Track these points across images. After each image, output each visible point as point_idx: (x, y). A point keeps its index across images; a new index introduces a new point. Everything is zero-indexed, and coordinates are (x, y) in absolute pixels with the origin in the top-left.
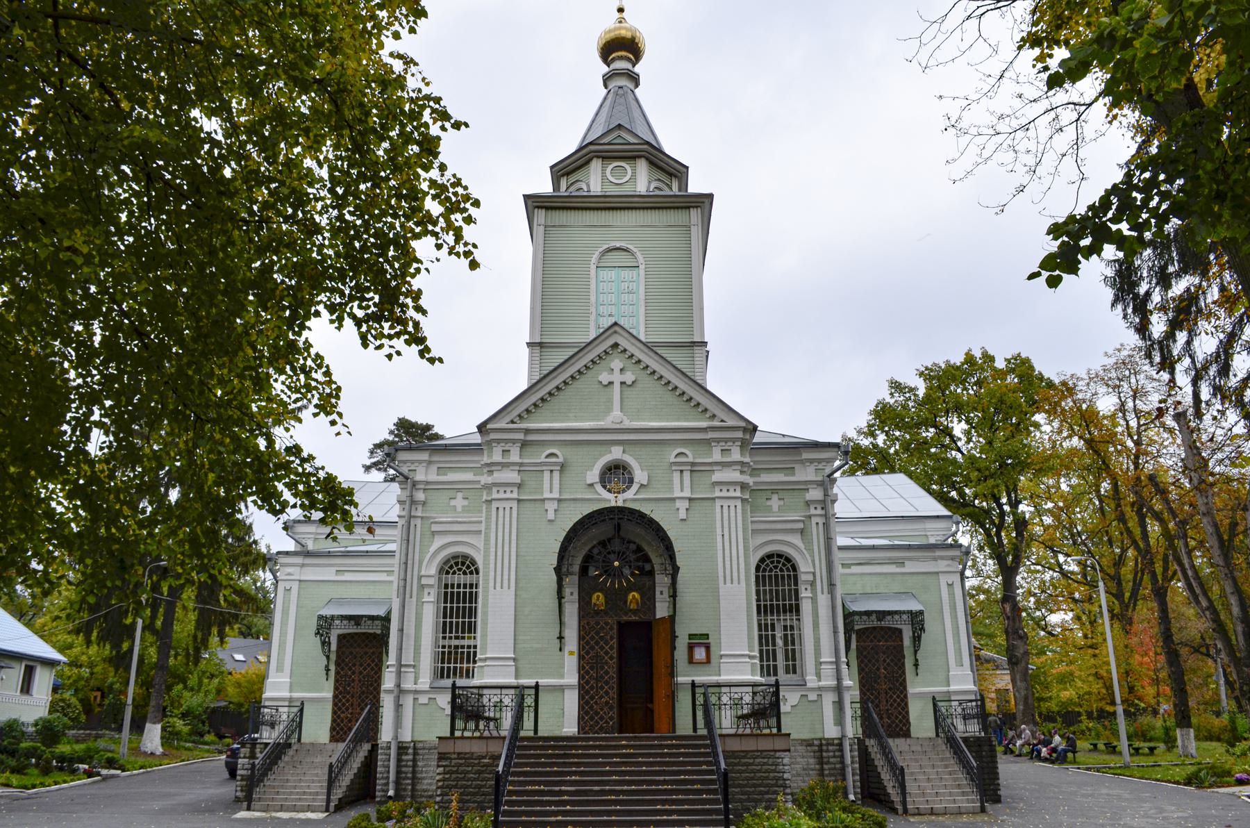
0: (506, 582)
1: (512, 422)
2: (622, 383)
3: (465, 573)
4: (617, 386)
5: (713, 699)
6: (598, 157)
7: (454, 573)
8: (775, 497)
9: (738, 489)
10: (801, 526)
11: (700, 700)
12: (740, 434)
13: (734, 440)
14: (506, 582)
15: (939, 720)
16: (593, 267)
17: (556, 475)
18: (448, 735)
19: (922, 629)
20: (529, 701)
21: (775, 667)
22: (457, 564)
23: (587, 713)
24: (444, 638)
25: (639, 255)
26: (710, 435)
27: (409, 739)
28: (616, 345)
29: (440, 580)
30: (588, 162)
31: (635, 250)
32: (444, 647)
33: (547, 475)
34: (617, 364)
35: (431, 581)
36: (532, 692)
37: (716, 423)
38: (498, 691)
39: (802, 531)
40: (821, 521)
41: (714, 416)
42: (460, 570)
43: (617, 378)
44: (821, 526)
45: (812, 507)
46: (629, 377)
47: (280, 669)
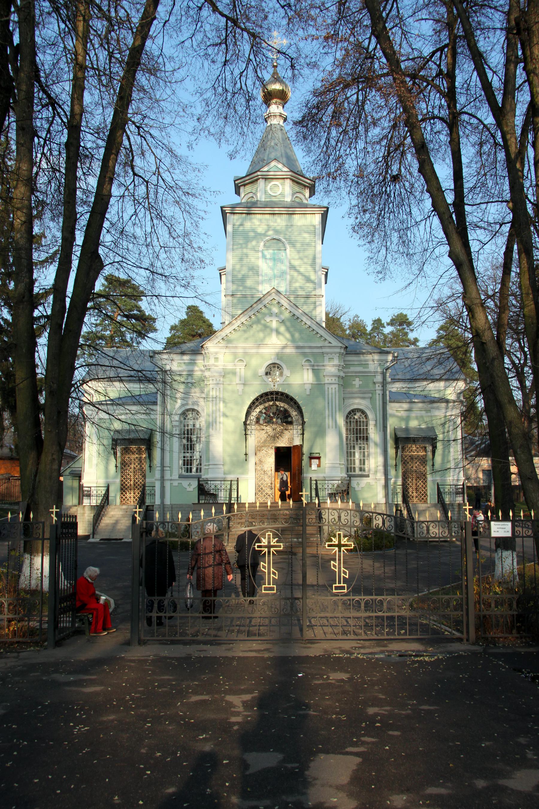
5: (320, 486)
6: (262, 178)
8: (357, 379)
9: (337, 379)
10: (370, 395)
11: (314, 486)
12: (338, 350)
13: (335, 353)
15: (440, 494)
18: (197, 502)
19: (436, 447)
20: (234, 487)
21: (354, 468)
23: (260, 491)
24: (184, 452)
26: (324, 350)
27: (169, 503)
29: (181, 422)
30: (257, 180)
31: (284, 240)
35: (177, 424)
36: (236, 482)
37: (326, 344)
38: (219, 482)
39: (371, 398)
40: (381, 392)
41: (325, 339)
44: (381, 395)
45: (377, 385)
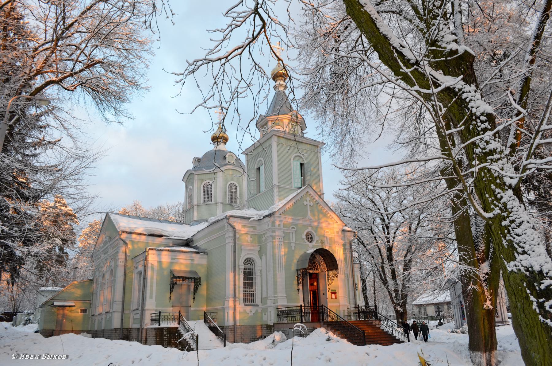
0: (282, 271)
1: (280, 214)
2: (310, 205)
3: (250, 265)
4: (308, 206)
7: (247, 264)
14: (282, 271)
16: (292, 161)
17: (294, 234)
22: (248, 261)
25: (304, 159)
28: (308, 192)
32: (245, 291)
33: (291, 234)
34: (308, 199)
42: (249, 263)
43: (308, 203)
46: (312, 204)
47: (151, 297)
